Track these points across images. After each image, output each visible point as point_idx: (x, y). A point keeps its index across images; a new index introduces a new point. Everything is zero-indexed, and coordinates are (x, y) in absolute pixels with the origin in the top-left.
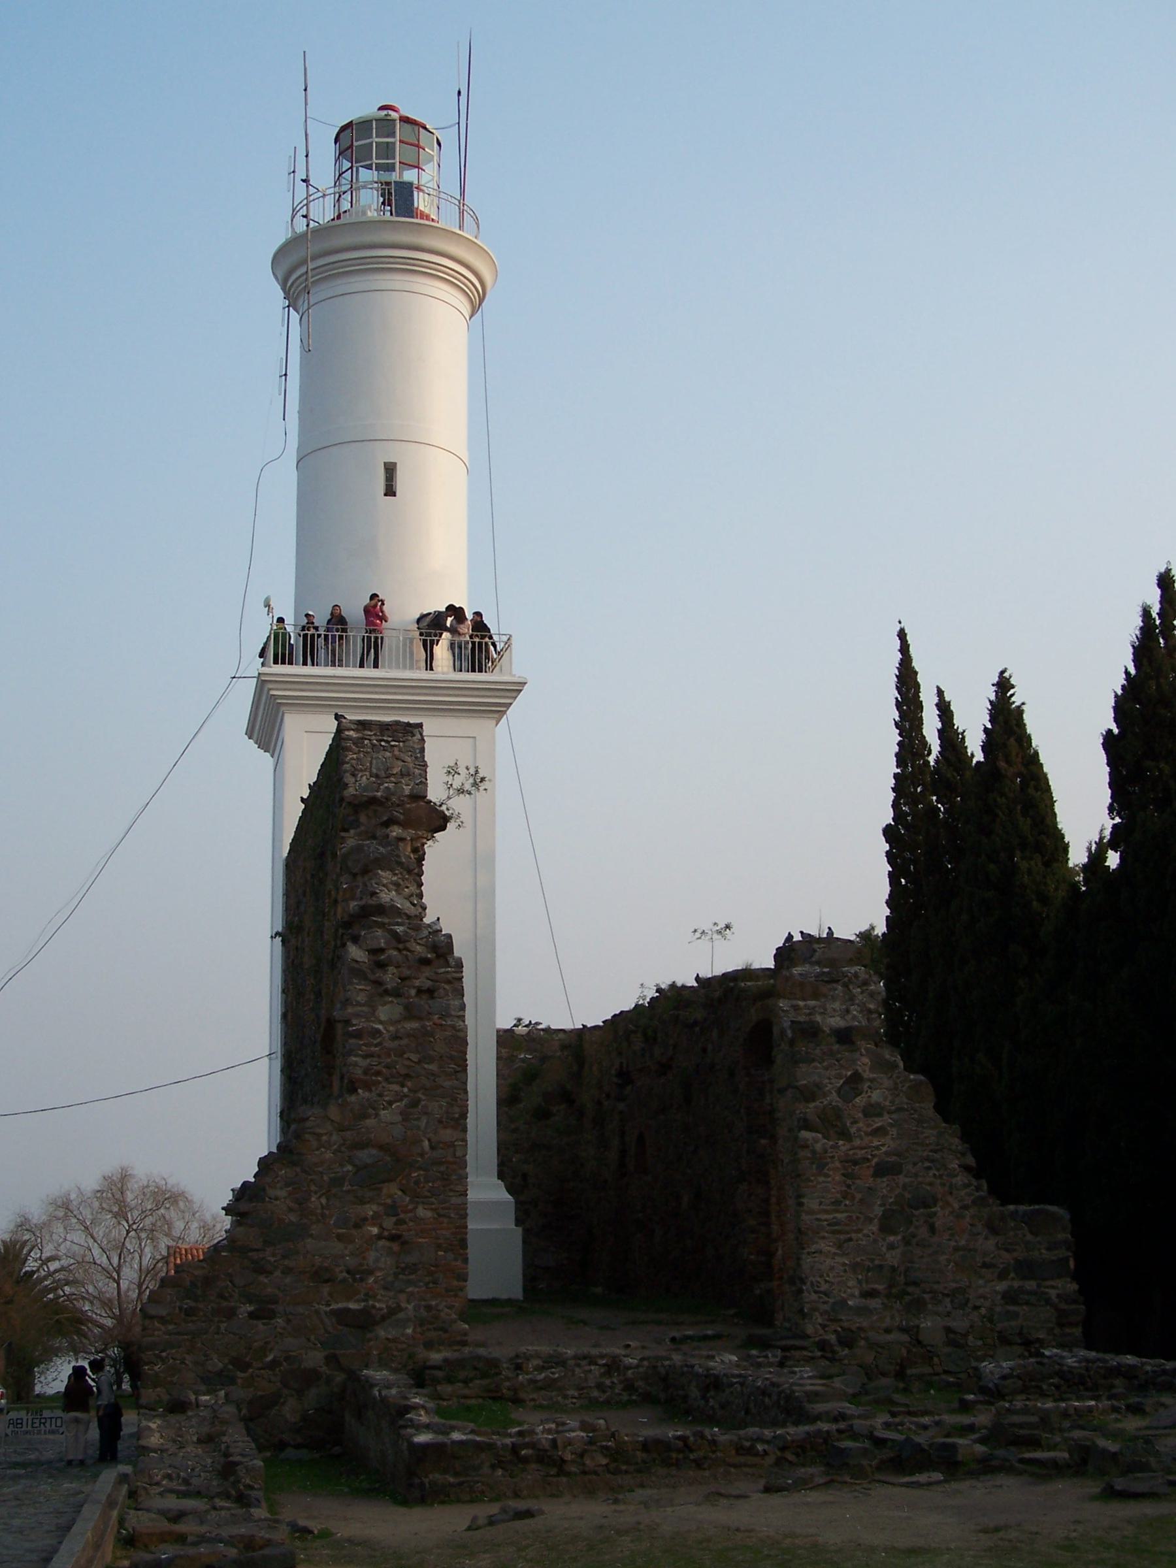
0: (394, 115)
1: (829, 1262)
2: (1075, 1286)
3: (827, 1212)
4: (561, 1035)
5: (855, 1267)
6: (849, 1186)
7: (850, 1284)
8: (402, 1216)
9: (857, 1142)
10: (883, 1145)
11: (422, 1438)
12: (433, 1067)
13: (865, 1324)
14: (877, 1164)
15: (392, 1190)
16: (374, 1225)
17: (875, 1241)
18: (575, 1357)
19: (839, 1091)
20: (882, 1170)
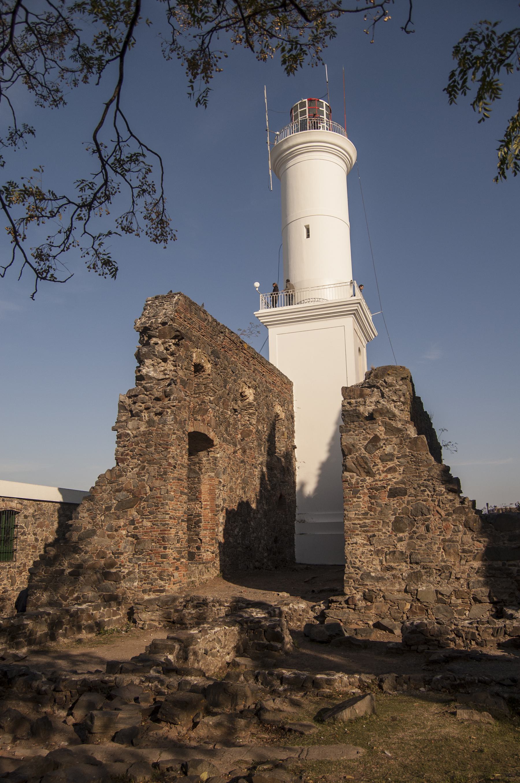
1: (361, 549)
3: (359, 519)
5: (378, 552)
6: (372, 504)
8: (137, 525)
9: (377, 477)
10: (394, 478)
12: (152, 449)
14: (390, 489)
15: (133, 513)
17: (390, 536)
20: (394, 493)
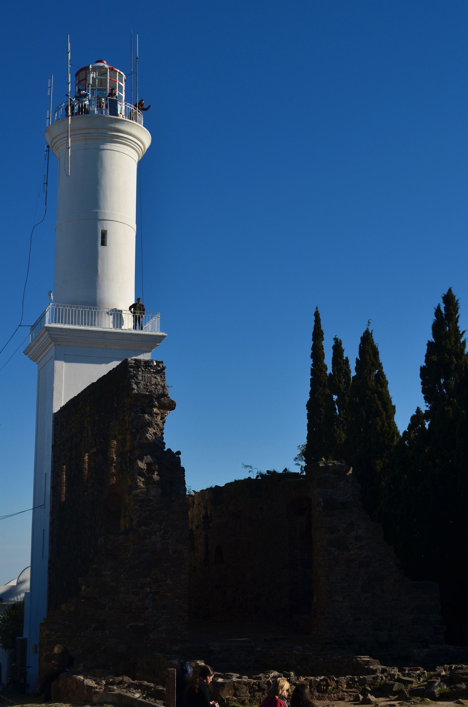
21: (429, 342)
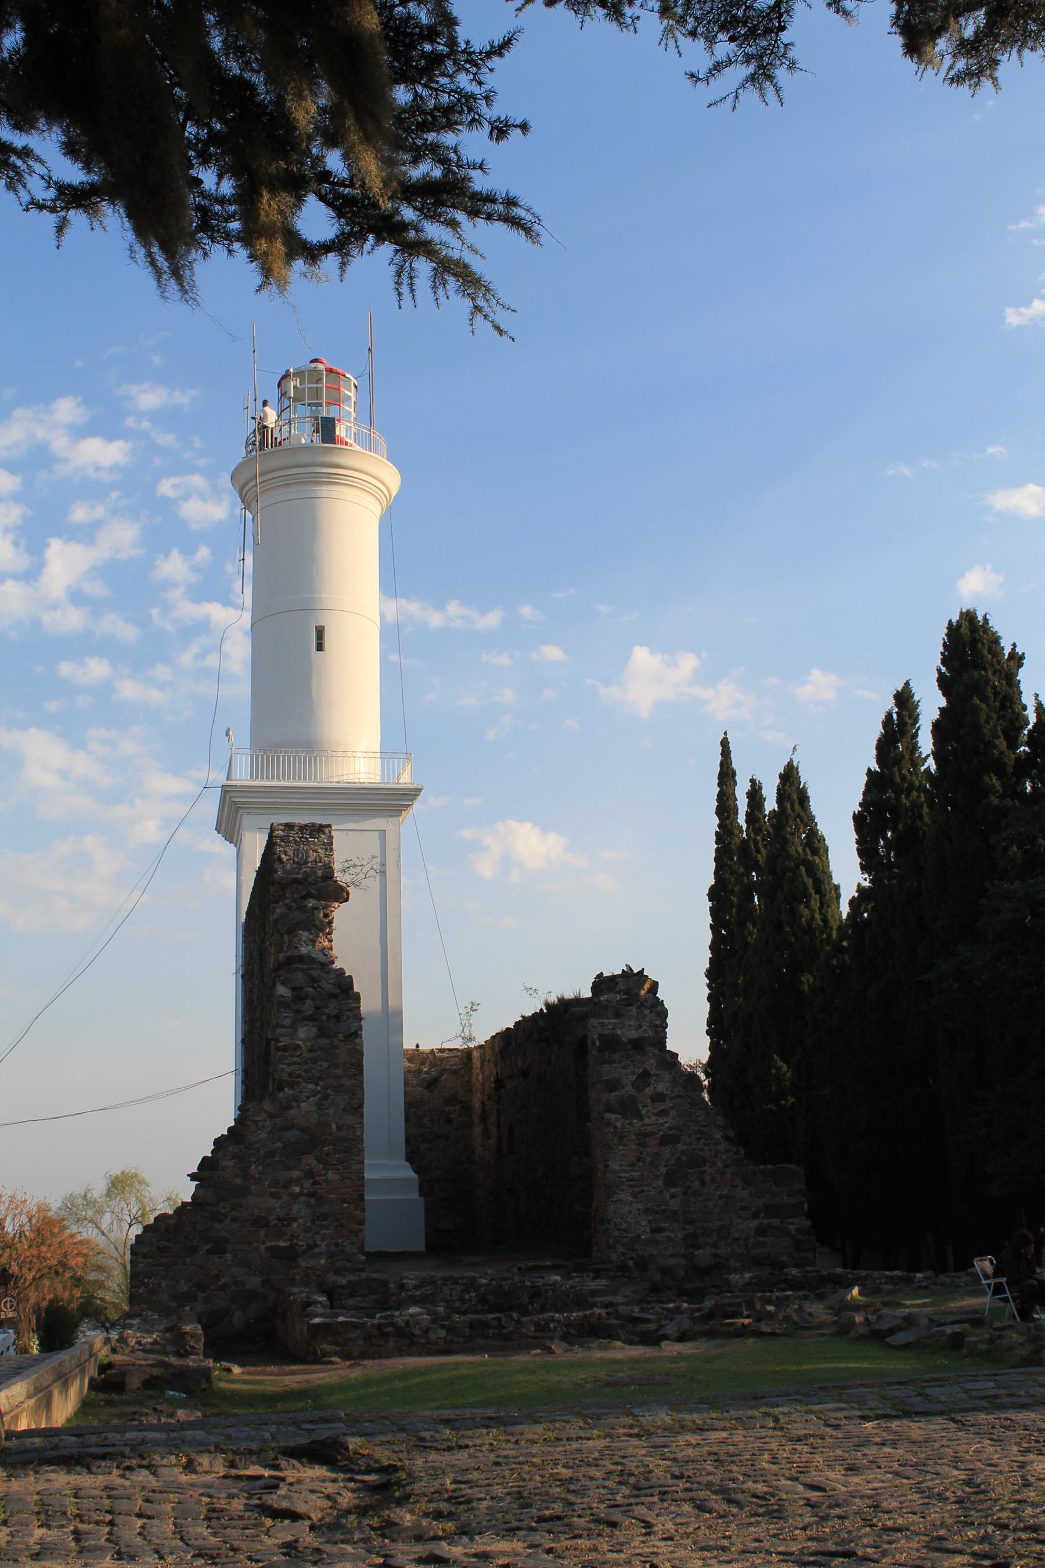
0: (321, 367)
2: (807, 1223)
3: (625, 1171)
4: (455, 1053)
5: (646, 1211)
6: (641, 1153)
7: (643, 1223)
8: (317, 1178)
9: (647, 1121)
11: (317, 1320)
12: (338, 1071)
13: (654, 1252)
16: (297, 1185)
17: (661, 1192)
18: (444, 1279)
19: (633, 1085)
20: (665, 1140)
21: (869, 770)
